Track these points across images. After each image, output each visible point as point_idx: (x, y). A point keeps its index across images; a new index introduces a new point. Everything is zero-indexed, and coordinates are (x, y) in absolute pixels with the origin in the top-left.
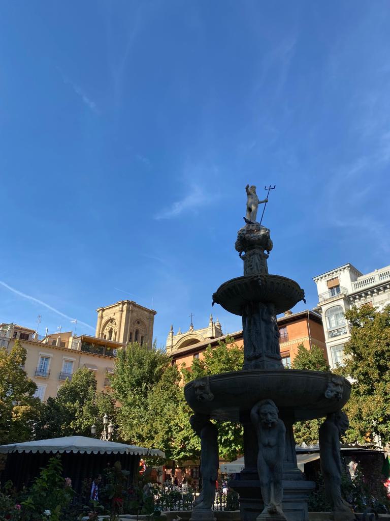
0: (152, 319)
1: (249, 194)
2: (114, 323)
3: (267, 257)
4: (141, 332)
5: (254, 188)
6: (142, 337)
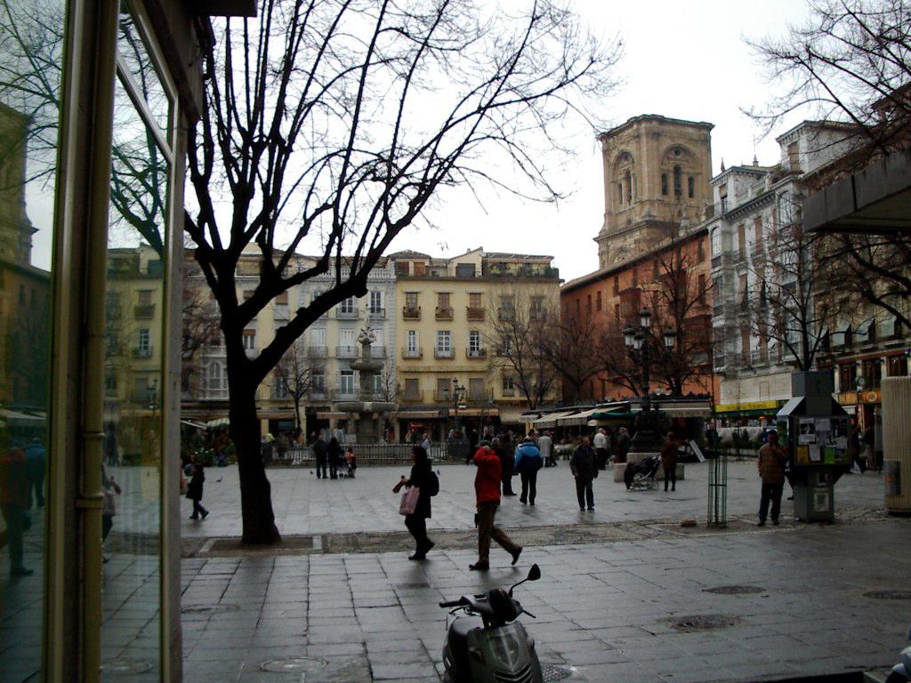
0: (706, 141)
4: (685, 170)
6: (691, 180)
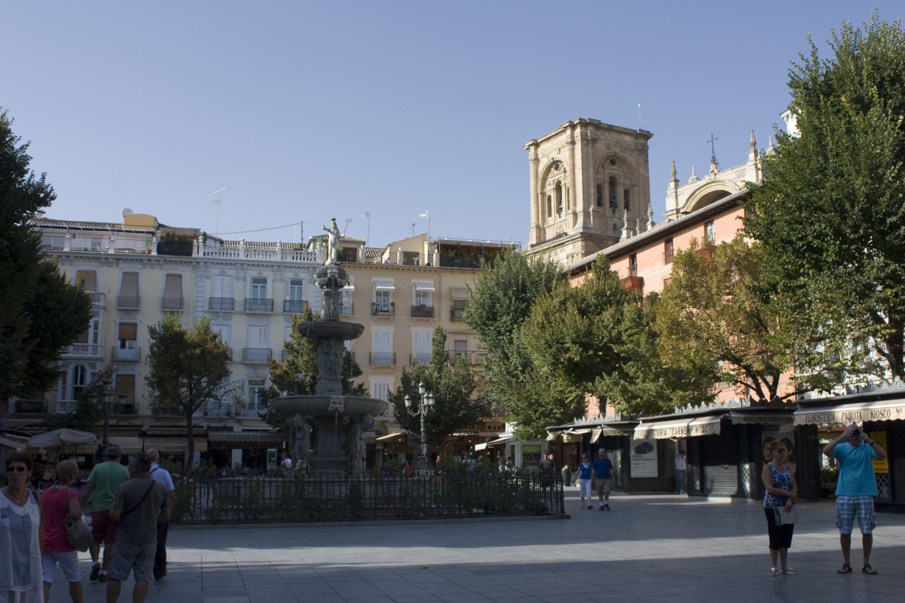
0: (643, 151)
2: (562, 169)
6: (626, 192)
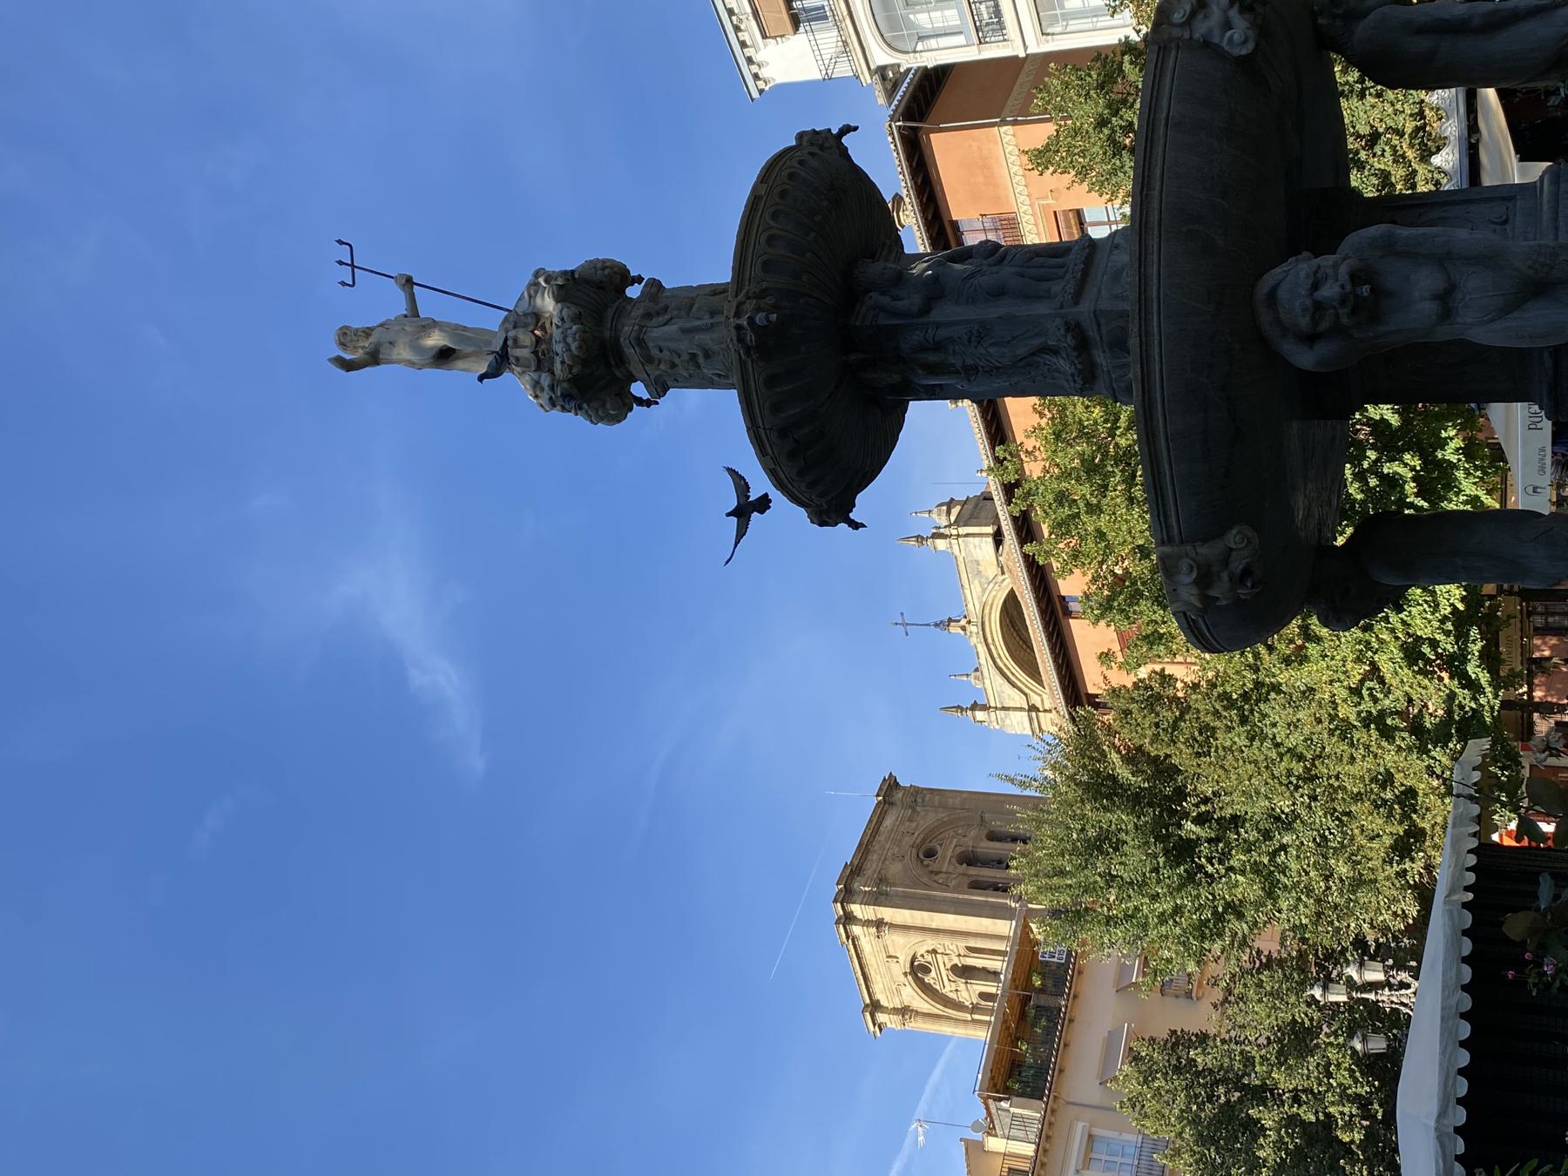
0: (918, 795)
1: (374, 358)
2: (929, 958)
3: (655, 285)
4: (969, 843)
5: (346, 336)
6: (993, 837)
